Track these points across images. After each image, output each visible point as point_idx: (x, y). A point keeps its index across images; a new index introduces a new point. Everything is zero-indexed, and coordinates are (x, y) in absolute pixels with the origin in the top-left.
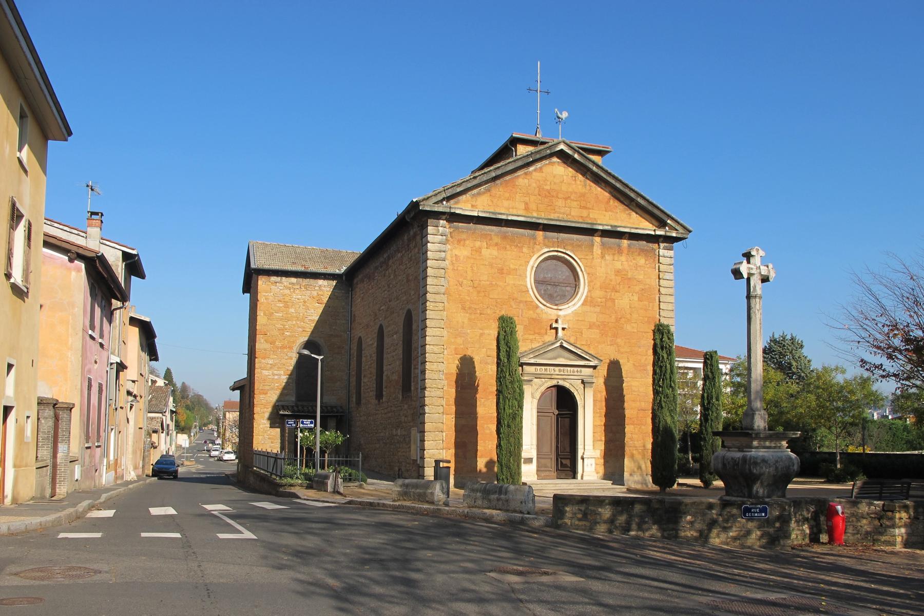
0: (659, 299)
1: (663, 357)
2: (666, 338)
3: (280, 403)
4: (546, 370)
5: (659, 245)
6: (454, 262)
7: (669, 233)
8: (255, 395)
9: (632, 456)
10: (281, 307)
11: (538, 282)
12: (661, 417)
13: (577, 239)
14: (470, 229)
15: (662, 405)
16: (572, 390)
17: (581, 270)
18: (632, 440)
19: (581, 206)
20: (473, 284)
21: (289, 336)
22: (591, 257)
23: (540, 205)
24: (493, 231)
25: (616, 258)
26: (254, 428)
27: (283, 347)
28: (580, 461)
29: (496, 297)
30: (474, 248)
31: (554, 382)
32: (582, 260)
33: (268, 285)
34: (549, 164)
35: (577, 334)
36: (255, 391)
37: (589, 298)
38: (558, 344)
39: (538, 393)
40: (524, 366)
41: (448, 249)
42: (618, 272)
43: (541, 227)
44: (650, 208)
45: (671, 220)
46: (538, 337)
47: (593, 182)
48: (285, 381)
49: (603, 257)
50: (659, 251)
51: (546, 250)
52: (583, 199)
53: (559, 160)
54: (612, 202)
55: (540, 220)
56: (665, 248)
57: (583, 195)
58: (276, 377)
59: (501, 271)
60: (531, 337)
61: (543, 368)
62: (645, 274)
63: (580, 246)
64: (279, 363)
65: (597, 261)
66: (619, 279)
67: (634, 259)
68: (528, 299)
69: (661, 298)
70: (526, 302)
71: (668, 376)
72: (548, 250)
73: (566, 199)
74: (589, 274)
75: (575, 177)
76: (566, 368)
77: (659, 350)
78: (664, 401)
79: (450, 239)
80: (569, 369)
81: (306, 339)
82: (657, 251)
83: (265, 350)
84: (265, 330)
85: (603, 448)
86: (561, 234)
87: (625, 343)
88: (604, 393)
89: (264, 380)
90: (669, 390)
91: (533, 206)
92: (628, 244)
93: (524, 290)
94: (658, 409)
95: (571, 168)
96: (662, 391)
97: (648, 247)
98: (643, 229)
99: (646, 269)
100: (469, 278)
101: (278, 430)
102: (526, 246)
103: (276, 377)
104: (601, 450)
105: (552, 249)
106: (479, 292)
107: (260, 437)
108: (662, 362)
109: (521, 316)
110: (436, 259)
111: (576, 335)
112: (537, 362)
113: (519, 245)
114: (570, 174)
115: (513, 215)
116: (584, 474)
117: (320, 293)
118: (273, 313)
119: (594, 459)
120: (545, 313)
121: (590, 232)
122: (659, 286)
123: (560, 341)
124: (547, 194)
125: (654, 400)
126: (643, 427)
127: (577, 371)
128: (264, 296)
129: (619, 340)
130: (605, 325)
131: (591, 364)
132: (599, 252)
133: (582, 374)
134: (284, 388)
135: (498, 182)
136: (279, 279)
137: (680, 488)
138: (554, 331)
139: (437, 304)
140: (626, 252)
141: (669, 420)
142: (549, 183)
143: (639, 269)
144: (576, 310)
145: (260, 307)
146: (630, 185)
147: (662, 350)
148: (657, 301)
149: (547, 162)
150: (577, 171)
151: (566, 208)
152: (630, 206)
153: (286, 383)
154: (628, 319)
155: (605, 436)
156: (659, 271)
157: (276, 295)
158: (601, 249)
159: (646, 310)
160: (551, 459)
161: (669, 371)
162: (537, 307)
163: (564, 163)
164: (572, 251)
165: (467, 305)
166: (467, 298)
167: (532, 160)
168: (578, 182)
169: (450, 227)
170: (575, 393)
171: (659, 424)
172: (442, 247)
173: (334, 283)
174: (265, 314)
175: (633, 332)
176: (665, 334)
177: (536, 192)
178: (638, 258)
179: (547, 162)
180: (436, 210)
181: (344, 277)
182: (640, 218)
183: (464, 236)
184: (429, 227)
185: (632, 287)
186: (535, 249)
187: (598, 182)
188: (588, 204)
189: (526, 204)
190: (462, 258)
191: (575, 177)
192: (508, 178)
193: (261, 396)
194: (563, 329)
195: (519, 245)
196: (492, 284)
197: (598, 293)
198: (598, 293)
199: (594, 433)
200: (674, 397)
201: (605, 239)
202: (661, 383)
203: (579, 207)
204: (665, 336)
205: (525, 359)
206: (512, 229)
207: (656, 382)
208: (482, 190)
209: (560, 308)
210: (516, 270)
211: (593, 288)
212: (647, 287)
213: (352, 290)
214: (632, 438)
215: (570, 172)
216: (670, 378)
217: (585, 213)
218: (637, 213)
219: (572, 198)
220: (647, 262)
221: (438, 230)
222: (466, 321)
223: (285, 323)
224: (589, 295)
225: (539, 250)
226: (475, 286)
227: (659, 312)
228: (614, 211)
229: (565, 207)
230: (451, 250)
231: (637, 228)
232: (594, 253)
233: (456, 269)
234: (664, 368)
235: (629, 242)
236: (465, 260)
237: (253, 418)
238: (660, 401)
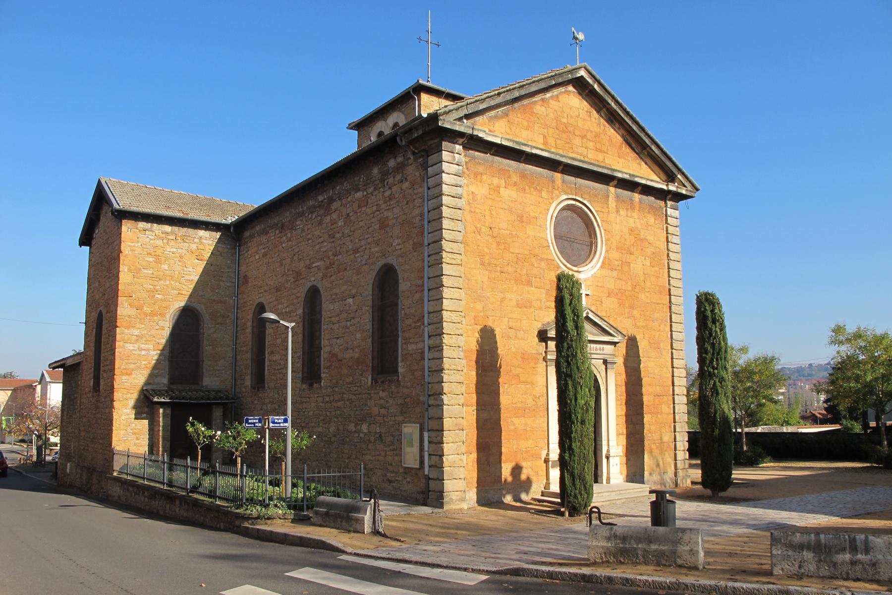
1: (716, 332)
3: (149, 387)
5: (666, 203)
6: (471, 202)
8: (115, 377)
9: (651, 452)
10: (151, 262)
11: (558, 237)
12: (717, 406)
17: (598, 225)
20: (492, 232)
21: (161, 300)
26: (114, 420)
27: (153, 314)
30: (492, 186)
33: (135, 232)
35: (597, 302)
36: (116, 370)
37: (607, 260)
42: (632, 230)
43: (561, 168)
44: (663, 158)
47: (606, 121)
48: (156, 357)
49: (618, 211)
50: (666, 210)
51: (565, 197)
52: (598, 140)
53: (574, 90)
57: (597, 135)
58: (143, 353)
59: (521, 218)
63: (596, 196)
64: (148, 334)
65: (613, 216)
68: (549, 257)
69: (670, 264)
70: (547, 260)
74: (605, 230)
81: (183, 304)
82: (664, 209)
83: (129, 316)
84: (130, 291)
86: (579, 179)
88: (624, 376)
89: (129, 356)
91: (551, 141)
93: (545, 245)
94: (712, 395)
95: (586, 101)
97: (657, 203)
101: (146, 422)
103: (143, 353)
104: (623, 445)
105: (570, 197)
106: (498, 243)
107: (122, 432)
111: (596, 304)
114: (586, 109)
117: (201, 247)
118: (140, 269)
119: (618, 458)
121: (605, 179)
126: (659, 416)
128: (129, 246)
129: (635, 312)
131: (616, 340)
133: (604, 352)
134: (155, 367)
135: (516, 105)
136: (149, 225)
140: (638, 208)
142: (565, 115)
143: (649, 228)
144: (595, 273)
145: (123, 261)
146: (647, 129)
148: (666, 267)
149: (562, 89)
150: (591, 106)
153: (157, 360)
156: (667, 233)
157: (145, 246)
163: (580, 94)
164: (589, 201)
165: (487, 259)
166: (485, 249)
168: (593, 120)
173: (218, 235)
174: (129, 270)
175: (647, 303)
177: (554, 125)
179: (563, 90)
181: (232, 228)
182: (649, 170)
185: (644, 249)
186: (554, 195)
187: (612, 122)
189: (545, 137)
192: (525, 102)
193: (124, 378)
195: (538, 188)
196: (512, 234)
197: (615, 255)
198: (615, 255)
199: (617, 425)
203: (594, 148)
206: (530, 166)
208: (499, 113)
209: (580, 269)
212: (657, 250)
213: (239, 246)
215: (585, 106)
217: (600, 157)
218: (646, 163)
219: (588, 137)
220: (656, 222)
222: (486, 280)
223: (156, 283)
225: (558, 197)
227: (669, 280)
229: (582, 147)
232: (610, 206)
236: (483, 200)
237: (112, 407)
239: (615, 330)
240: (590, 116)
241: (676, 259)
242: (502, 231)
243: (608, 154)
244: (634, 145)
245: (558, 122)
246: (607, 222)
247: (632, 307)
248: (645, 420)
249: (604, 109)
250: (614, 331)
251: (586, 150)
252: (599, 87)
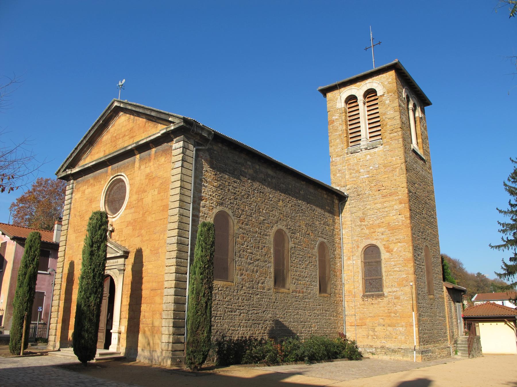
7: (168, 129)
9: (144, 332)
87: (147, 232)
98: (154, 135)
126: (152, 306)
133: (118, 264)
137: (98, 361)
152: (157, 121)
159: (162, 200)
185: (154, 184)
218: (161, 124)
231: (150, 137)
247: (141, 229)
248: (142, 308)
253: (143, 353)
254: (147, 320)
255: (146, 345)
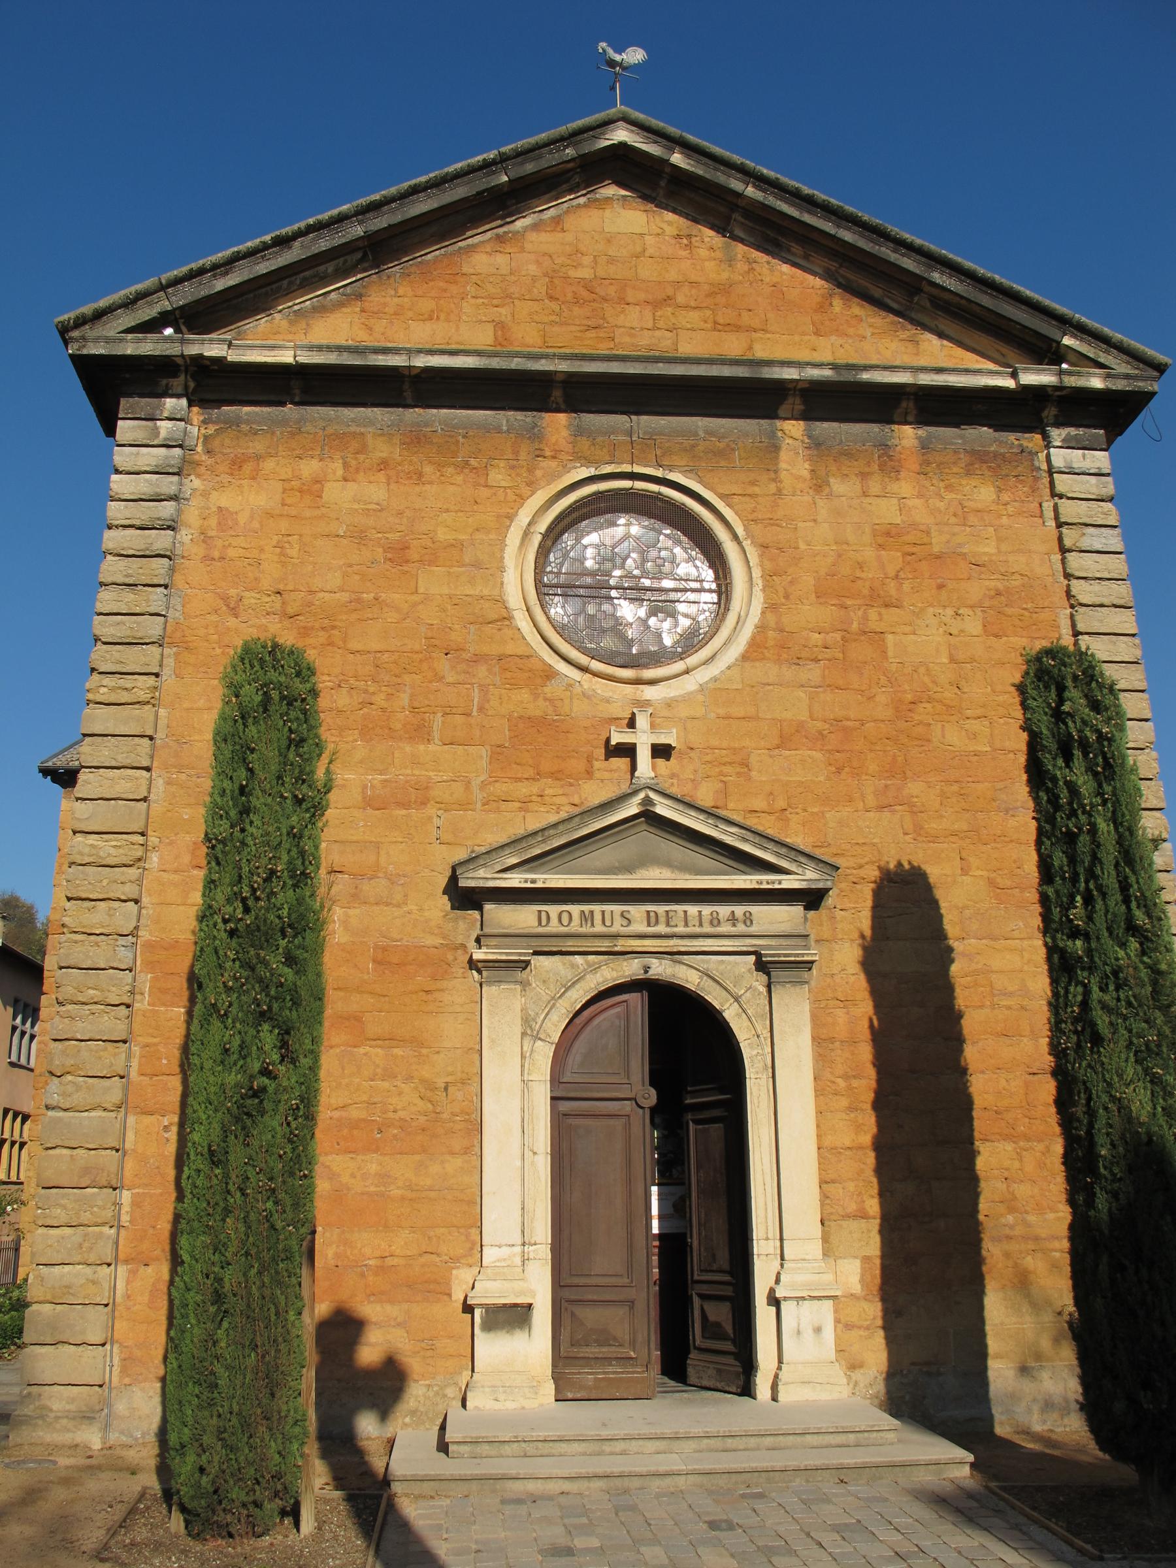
0: (1074, 625)
2: (1075, 700)
4: (587, 918)
5: (1046, 437)
7: (1073, 378)
12: (1098, 1089)
13: (710, 433)
14: (284, 422)
15: (1093, 1025)
16: (714, 997)
17: (735, 537)
18: (1012, 1210)
19: (715, 323)
22: (772, 487)
23: (556, 329)
24: (371, 423)
25: (875, 486)
28: (763, 1315)
29: (375, 645)
31: (630, 969)
32: (736, 499)
34: (585, 206)
35: (728, 769)
37: (771, 634)
38: (632, 808)
39: (554, 1016)
40: (488, 907)
41: (194, 490)
42: (887, 536)
44: (986, 300)
45: (1074, 336)
46: (551, 788)
47: (759, 248)
49: (819, 485)
50: (1048, 456)
54: (837, 304)
55: (543, 361)
56: (1068, 445)
57: (723, 289)
59: (399, 554)
60: (523, 789)
61: (575, 909)
62: (1000, 540)
63: (720, 454)
66: (893, 560)
67: (949, 488)
68: (510, 649)
69: (1078, 618)
71: (1110, 879)
72: (592, 472)
73: (656, 305)
74: (765, 547)
75: (689, 236)
76: (679, 908)
77: (1054, 765)
78: (1104, 1006)
79: (204, 458)
80: (693, 909)
82: (1042, 456)
85: (873, 1246)
86: (644, 418)
87: (943, 795)
90: (1123, 945)
92: (919, 438)
93: (493, 616)
94: (1079, 1046)
96: (1089, 952)
99: (1005, 520)
100: (266, 584)
102: (502, 464)
104: (866, 1259)
105: (608, 469)
108: (1073, 813)
109: (481, 709)
110: (138, 523)
111: (721, 774)
112: (539, 885)
113: (473, 462)
114: (670, 231)
115: (431, 352)
116: (782, 1375)
120: (584, 694)
122: (1067, 576)
123: (642, 795)
124: (585, 294)
125: (1057, 1004)
127: (733, 919)
129: (914, 788)
130: (845, 729)
132: (803, 469)
133: (754, 929)
138: (622, 763)
139: (127, 682)
140: (915, 467)
141: (1140, 1101)
142: (587, 260)
143: (973, 519)
144: (715, 679)
146: (893, 229)
147: (1068, 759)
151: (658, 333)
154: (948, 707)
155: (881, 1194)
156: (1059, 525)
158: (810, 459)
160: (631, 1303)
161: (1110, 853)
162: (550, 674)
163: (646, 198)
164: (685, 473)
167: (506, 179)
168: (703, 252)
169: (204, 422)
170: (730, 1014)
171: (1091, 1125)
172: (168, 485)
176: (1069, 683)
177: (540, 289)
178: (968, 484)
179: (582, 200)
180: (129, 352)
183: (258, 446)
184: (120, 423)
185: (951, 585)
186: (539, 473)
187: (778, 245)
188: (745, 314)
190: (242, 519)
191: (689, 236)
194: (661, 752)
195: (473, 462)
199: (823, 1182)
200: (1155, 983)
201: (826, 425)
202: (1077, 912)
204: (1073, 693)
205: (481, 873)
206: (444, 411)
207: (1056, 911)
210: (458, 546)
211: (787, 597)
212: (1016, 582)
214: (1015, 1198)
215: (670, 223)
216: (1124, 887)
217: (733, 346)
218: (941, 335)
219: (680, 299)
220: (1005, 497)
221: (156, 432)
224: (771, 619)
225: (553, 477)
226: (291, 610)
228: (851, 331)
230: (205, 494)
231: (940, 370)
232: (783, 475)
233: (216, 554)
234: (1084, 839)
235: (922, 432)
238: (1085, 1005)
239: (783, 851)
240: (689, 246)
241: (1106, 601)
242: (321, 595)
243: (765, 331)
244: (877, 293)
245: (556, 281)
246: (773, 522)
248: (980, 1163)
249: (736, 216)
250: (778, 854)
251: (668, 334)
252: (688, 157)
253: (1027, 1387)
254: (1031, 1218)
255: (1045, 1344)
